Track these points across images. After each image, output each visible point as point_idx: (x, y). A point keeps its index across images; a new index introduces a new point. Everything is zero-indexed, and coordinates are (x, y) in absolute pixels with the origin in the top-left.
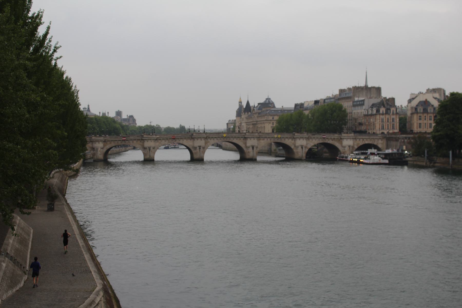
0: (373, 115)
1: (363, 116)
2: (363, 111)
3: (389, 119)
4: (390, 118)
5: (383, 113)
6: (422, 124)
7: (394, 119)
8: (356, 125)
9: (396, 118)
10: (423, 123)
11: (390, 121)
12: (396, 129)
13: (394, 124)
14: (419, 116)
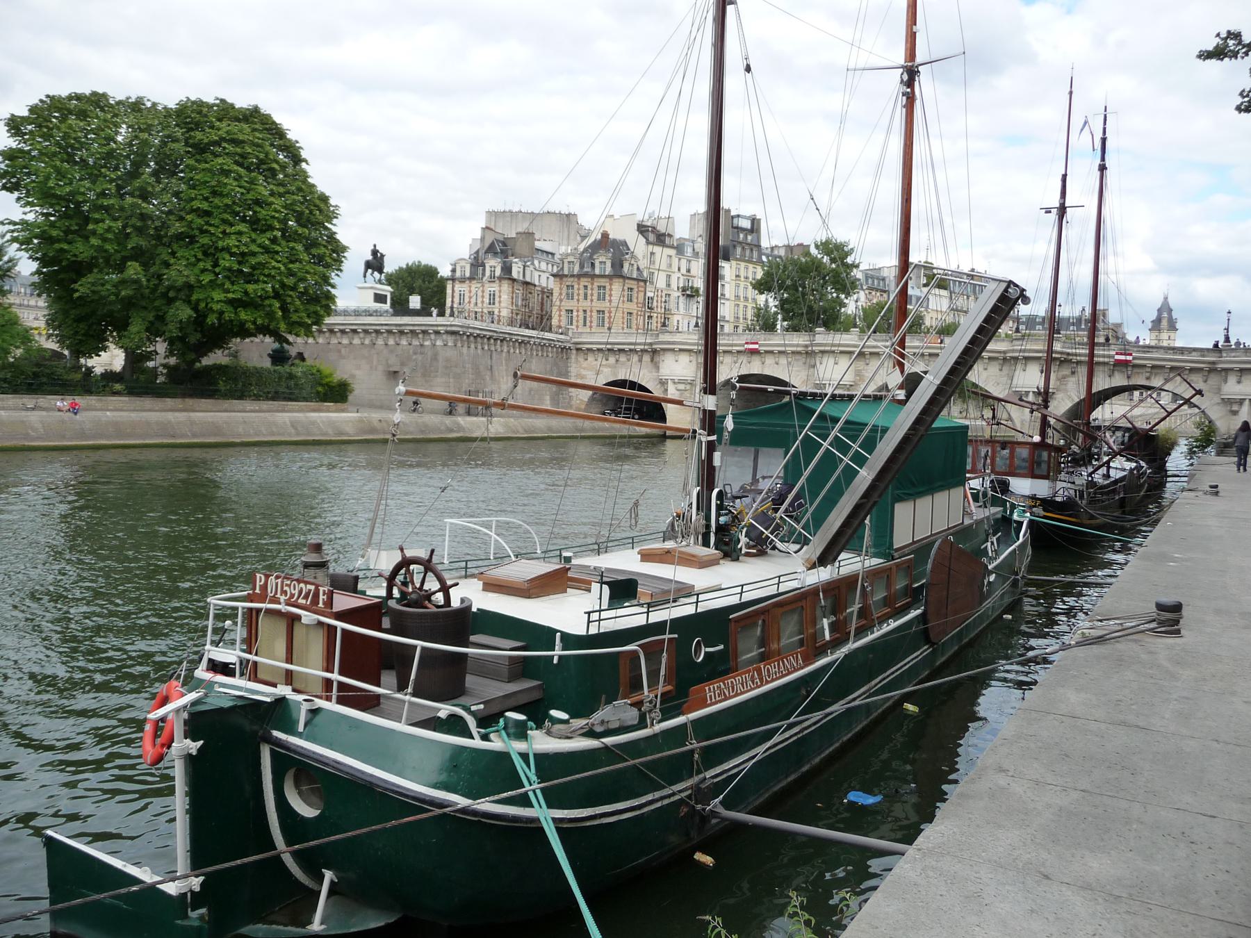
3: (480, 294)
4: (483, 292)
6: (575, 314)
7: (494, 295)
9: (500, 291)
10: (578, 311)
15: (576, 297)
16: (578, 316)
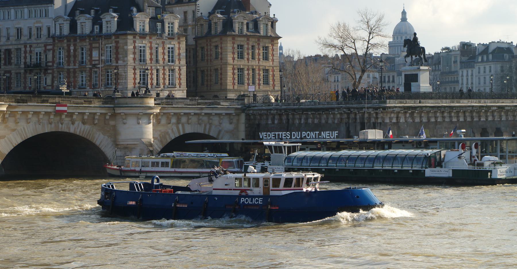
0: (108, 36)
1: (50, 41)
2: (46, 23)
3: (160, 50)
5: (143, 30)
6: (246, 72)
7: (172, 52)
8: (9, 72)
11: (164, 59)
12: (180, 84)
13: (173, 70)
14: (238, 46)
15: (246, 56)
16: (248, 74)
